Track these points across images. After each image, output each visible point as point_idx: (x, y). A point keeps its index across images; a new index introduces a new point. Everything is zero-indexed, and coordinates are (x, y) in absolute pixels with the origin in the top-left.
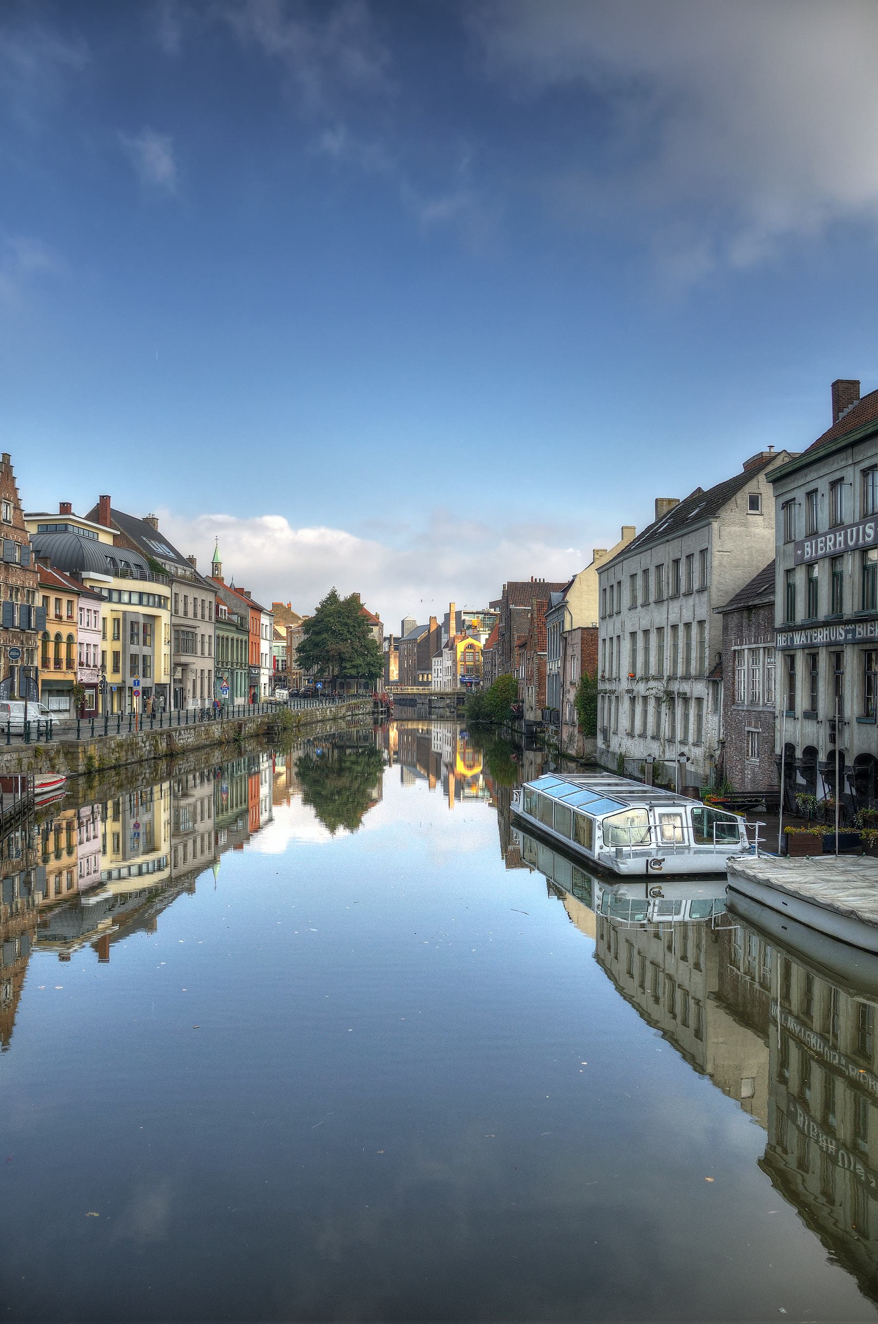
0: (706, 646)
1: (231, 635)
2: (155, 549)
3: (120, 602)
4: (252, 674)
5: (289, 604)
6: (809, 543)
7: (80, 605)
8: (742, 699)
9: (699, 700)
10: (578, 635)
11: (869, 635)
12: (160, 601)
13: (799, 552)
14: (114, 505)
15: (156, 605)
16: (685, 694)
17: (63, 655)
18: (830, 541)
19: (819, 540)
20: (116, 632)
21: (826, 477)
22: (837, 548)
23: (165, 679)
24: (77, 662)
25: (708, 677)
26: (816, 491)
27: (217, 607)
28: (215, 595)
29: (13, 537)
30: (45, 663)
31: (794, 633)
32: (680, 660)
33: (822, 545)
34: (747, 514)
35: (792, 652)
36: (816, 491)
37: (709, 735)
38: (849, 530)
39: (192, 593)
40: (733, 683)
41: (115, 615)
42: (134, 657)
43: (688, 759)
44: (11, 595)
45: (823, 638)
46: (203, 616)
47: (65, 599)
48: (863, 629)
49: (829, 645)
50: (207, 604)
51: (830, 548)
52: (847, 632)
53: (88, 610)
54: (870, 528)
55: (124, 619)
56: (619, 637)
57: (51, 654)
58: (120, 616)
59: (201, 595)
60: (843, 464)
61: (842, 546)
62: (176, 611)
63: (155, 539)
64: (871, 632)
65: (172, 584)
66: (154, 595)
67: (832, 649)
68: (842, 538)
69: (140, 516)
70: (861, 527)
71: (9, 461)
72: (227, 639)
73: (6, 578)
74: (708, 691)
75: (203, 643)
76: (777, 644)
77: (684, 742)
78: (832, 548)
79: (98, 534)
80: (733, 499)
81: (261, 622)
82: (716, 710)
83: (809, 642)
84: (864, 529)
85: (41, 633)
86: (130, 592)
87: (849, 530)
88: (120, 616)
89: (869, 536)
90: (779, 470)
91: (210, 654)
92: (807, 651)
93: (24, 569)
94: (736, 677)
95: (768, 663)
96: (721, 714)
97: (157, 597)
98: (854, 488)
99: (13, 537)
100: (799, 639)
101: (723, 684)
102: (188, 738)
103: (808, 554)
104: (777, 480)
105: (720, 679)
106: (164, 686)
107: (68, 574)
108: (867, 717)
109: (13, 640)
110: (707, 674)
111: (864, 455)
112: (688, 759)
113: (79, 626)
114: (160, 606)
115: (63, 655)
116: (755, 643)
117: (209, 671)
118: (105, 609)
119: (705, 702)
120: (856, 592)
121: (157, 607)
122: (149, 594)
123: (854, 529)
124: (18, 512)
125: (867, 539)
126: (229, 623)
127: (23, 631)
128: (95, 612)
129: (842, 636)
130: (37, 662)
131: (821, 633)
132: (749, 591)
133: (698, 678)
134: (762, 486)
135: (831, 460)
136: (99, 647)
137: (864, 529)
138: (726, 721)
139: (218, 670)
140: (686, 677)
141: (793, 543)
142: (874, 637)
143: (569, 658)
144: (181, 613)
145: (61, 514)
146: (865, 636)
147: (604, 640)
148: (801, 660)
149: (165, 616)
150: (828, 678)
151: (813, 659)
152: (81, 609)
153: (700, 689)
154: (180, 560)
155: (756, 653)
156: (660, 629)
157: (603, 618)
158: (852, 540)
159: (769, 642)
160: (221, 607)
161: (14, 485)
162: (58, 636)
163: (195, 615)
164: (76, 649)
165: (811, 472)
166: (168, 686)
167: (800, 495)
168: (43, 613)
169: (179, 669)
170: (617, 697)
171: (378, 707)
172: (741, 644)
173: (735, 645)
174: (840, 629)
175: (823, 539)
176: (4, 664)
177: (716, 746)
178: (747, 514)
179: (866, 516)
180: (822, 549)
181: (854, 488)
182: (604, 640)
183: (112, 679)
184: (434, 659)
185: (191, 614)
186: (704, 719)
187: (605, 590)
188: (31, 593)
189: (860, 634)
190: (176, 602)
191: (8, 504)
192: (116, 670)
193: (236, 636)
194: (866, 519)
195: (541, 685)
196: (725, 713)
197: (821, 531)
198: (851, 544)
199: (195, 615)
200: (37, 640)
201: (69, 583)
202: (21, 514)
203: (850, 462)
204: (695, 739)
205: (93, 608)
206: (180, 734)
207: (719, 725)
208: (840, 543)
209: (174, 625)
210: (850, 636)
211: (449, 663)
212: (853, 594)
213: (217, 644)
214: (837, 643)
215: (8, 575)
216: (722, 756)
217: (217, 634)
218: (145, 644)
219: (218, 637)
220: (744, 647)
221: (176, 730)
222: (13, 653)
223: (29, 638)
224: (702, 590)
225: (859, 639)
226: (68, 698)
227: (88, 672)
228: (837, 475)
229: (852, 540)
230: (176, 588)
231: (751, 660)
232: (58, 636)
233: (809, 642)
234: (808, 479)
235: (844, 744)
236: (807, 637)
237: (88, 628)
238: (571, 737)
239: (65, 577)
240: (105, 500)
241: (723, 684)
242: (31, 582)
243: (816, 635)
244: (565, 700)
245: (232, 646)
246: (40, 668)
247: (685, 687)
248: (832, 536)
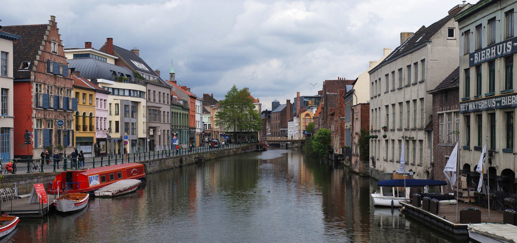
0: (424, 112)
1: (179, 111)
2: (137, 66)
3: (118, 95)
4: (191, 131)
5: (212, 95)
6: (477, 54)
7: (97, 97)
8: (443, 140)
9: (421, 141)
10: (359, 108)
11: (509, 104)
12: (141, 94)
13: (472, 59)
14: (115, 43)
15: (138, 96)
16: (413, 138)
17: (88, 123)
18: (488, 52)
19: (482, 52)
20: (117, 111)
21: (486, 17)
22: (492, 56)
23: (143, 136)
24: (95, 127)
25: (425, 129)
26: (481, 25)
27: (172, 96)
28: (171, 90)
29: (58, 61)
30: (77, 128)
31: (469, 103)
32: (411, 120)
33: (484, 55)
34: (447, 39)
35: (468, 114)
36: (481, 25)
37: (426, 160)
38: (498, 46)
39: (158, 89)
40: (438, 132)
41: (116, 102)
42: (127, 124)
43: (414, 173)
44: (58, 92)
46: (164, 102)
47: (88, 93)
48: (505, 100)
49: (487, 109)
50: (166, 95)
51: (488, 56)
52: (497, 102)
53: (101, 100)
54: (510, 44)
55: (121, 104)
56: (380, 108)
57: (81, 123)
58: (119, 102)
59: (163, 90)
60: (495, 9)
61: (494, 55)
62: (149, 99)
63: (137, 61)
64: (510, 102)
65: (147, 85)
66: (137, 91)
67: (490, 112)
68: (494, 51)
69: (129, 49)
70: (504, 44)
71: (54, 20)
72: (177, 113)
73: (55, 83)
74: (425, 136)
75: (164, 116)
76: (460, 110)
77: (413, 165)
78: (489, 56)
79: (106, 59)
80: (439, 31)
81: (196, 104)
82: (430, 147)
83: (477, 108)
84: (506, 45)
85: (75, 113)
86: (124, 90)
87: (498, 46)
88: (119, 102)
90: (461, 15)
91: (168, 122)
92: (476, 113)
93: (65, 78)
94: (440, 128)
95: (457, 120)
96: (432, 149)
97: (138, 92)
98: (501, 22)
99: (58, 61)
101: (433, 133)
102: (155, 166)
103: (476, 60)
104: (460, 21)
105: (431, 129)
106: (143, 139)
107: (90, 80)
108: (509, 148)
109: (59, 116)
110: (425, 127)
111: (507, 4)
112: (414, 173)
113: (96, 108)
114: (140, 97)
115: (88, 123)
116: (449, 110)
117: (168, 131)
118: (110, 99)
119: (424, 142)
120: (502, 80)
121: (138, 97)
122: (134, 91)
123: (501, 45)
124: (61, 47)
125: (508, 50)
126: (179, 105)
127: (65, 111)
128: (105, 100)
129: (494, 104)
130: (73, 127)
131: (483, 103)
132: (447, 81)
133: (420, 129)
134: (453, 24)
135: (489, 8)
136: (107, 119)
137: (506, 45)
138: (434, 152)
139: (172, 130)
140: (414, 129)
141: (468, 55)
142: (511, 105)
143: (355, 120)
144: (152, 100)
145: (86, 48)
146: (506, 104)
147: (372, 110)
148: (473, 118)
149: (143, 102)
150: (487, 128)
151: (479, 118)
152: (97, 99)
153: (421, 135)
154: (151, 72)
155: (450, 115)
156: (401, 104)
157: (372, 98)
158: (499, 51)
159: (457, 109)
160: (173, 96)
161: (58, 33)
162: (84, 113)
163: (160, 101)
164: (94, 120)
165: (478, 15)
166: (146, 139)
167: (472, 28)
168: (76, 102)
169: (152, 130)
170: (379, 140)
171: (259, 149)
172: (442, 110)
173: (439, 111)
174: (493, 100)
175: (484, 51)
176: (55, 129)
177: (429, 166)
178: (447, 39)
179: (510, 38)
180: (484, 57)
181: (501, 22)
182: (372, 110)
183: (115, 135)
184: (289, 123)
185: (157, 101)
186: (423, 151)
187: (373, 83)
188: (69, 90)
189: (504, 103)
190: (149, 94)
191: (55, 43)
192: (117, 131)
193: (182, 112)
194: (508, 39)
195: (342, 135)
196: (434, 148)
197: (483, 47)
198: (499, 53)
199: (160, 101)
200: (73, 116)
201: (90, 85)
202: (62, 48)
203: (499, 8)
204: (419, 162)
205: (104, 98)
206: (150, 164)
207: (431, 155)
209: (148, 107)
210: (498, 104)
211: (297, 124)
212: (500, 81)
213: (172, 116)
214: (491, 109)
215: (56, 81)
216: (432, 171)
217: (172, 111)
218: (132, 116)
219: (172, 113)
220: (443, 112)
221: (147, 162)
222: (60, 123)
223: (68, 115)
224: (421, 82)
225: (503, 106)
226: (91, 146)
227: (102, 132)
228: (492, 16)
229: (499, 51)
230: (150, 87)
231: (447, 119)
232: (84, 113)
233: (477, 108)
234: (477, 18)
235: (496, 164)
236: (476, 105)
237: (101, 109)
238: (356, 162)
239: (88, 82)
240: (110, 40)
241: (433, 133)
242: (69, 85)
243: (480, 104)
244: (353, 143)
245: (180, 117)
246: (75, 131)
247: (413, 134)
248: (489, 50)
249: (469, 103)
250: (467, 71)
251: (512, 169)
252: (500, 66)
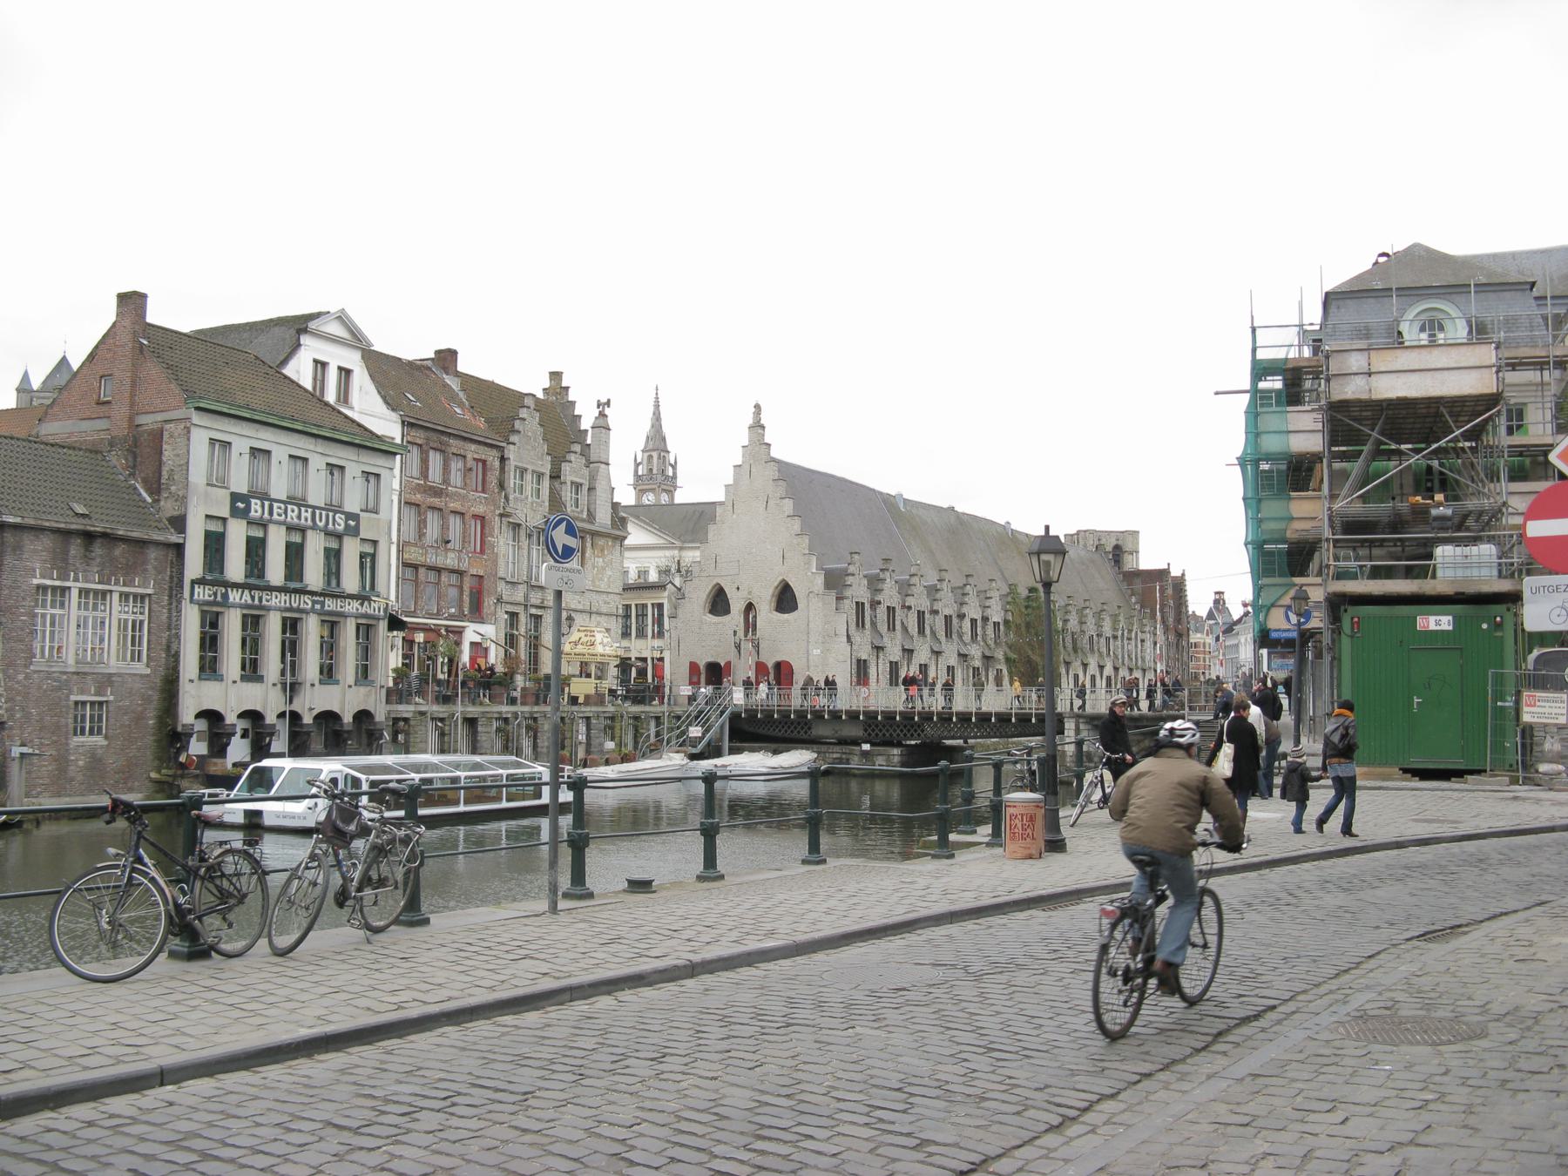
11: (339, 609)
45: (280, 602)
52: (314, 602)
64: (341, 607)
83: (256, 602)
89: (339, 525)
142: (343, 612)
158: (321, 520)
173: (43, 577)
208: (306, 519)
229: (321, 520)
233: (256, 602)
249: (229, 590)
251: (336, 709)
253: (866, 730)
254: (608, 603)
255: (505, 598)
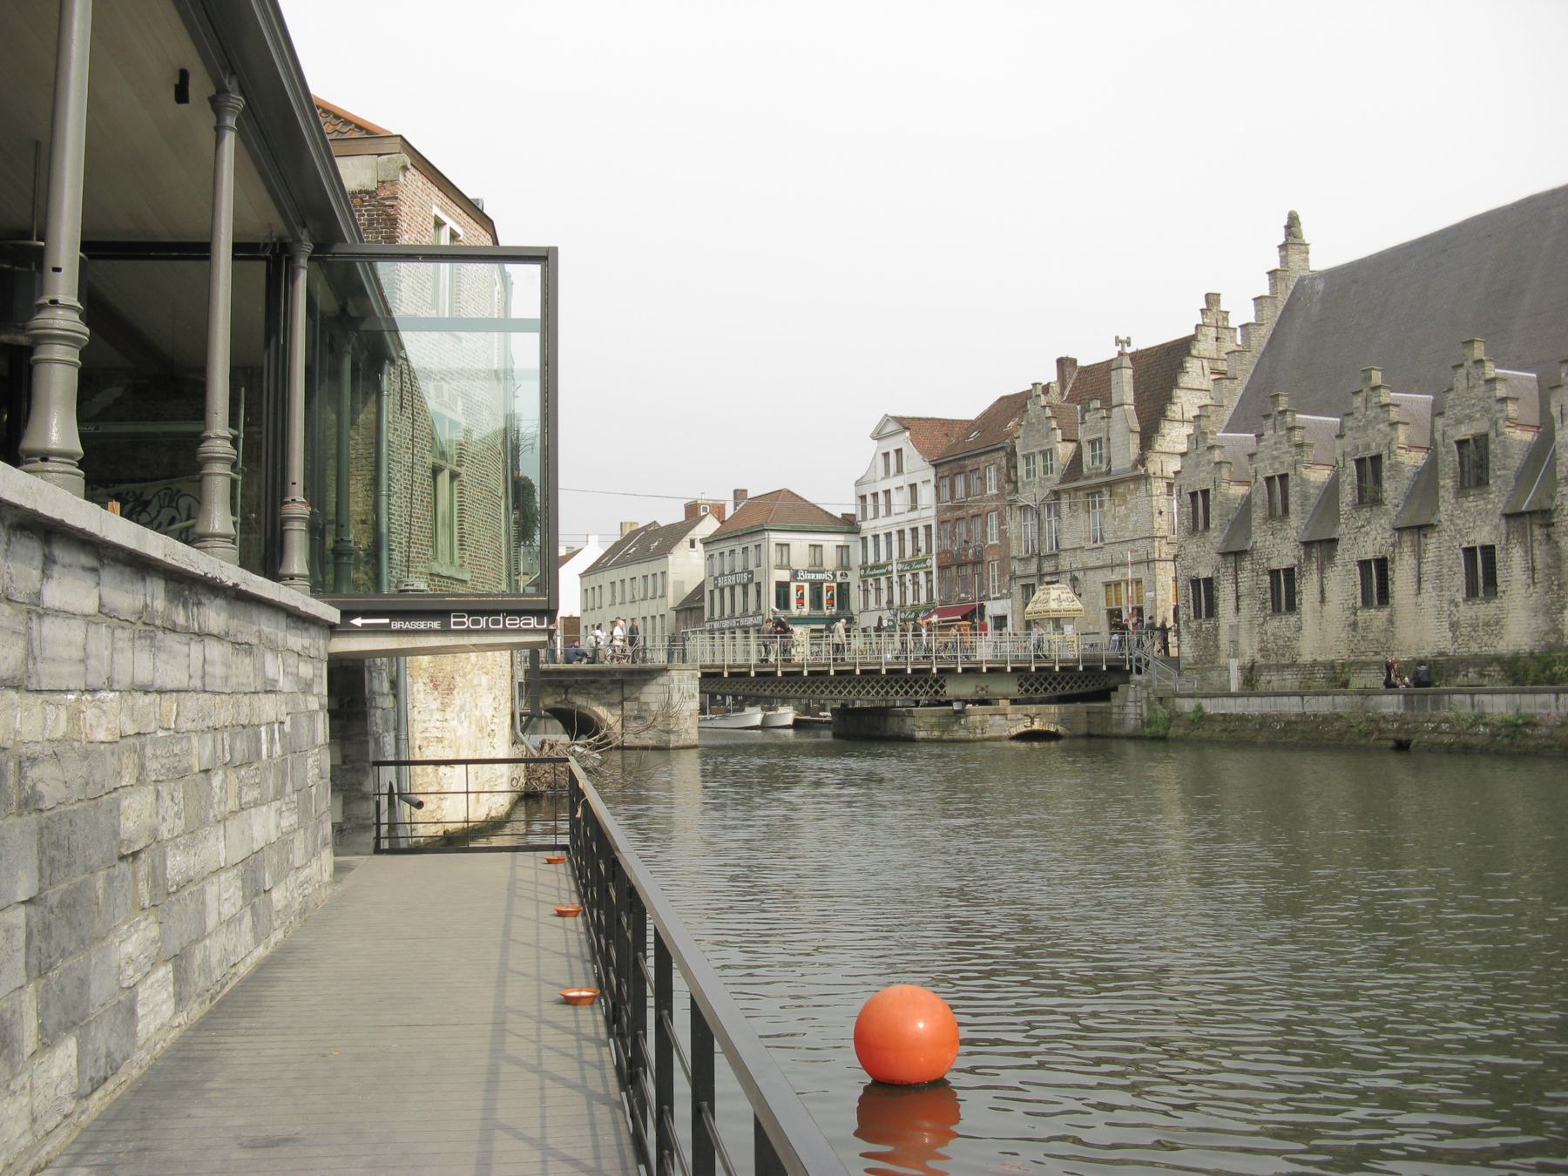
100: (716, 625)
147: (586, 627)
157: (585, 611)
182: (586, 627)
187: (586, 590)
224: (662, 597)
250: (712, 592)
252: (739, 591)
253: (1021, 686)
254: (1137, 551)
255: (1018, 573)
